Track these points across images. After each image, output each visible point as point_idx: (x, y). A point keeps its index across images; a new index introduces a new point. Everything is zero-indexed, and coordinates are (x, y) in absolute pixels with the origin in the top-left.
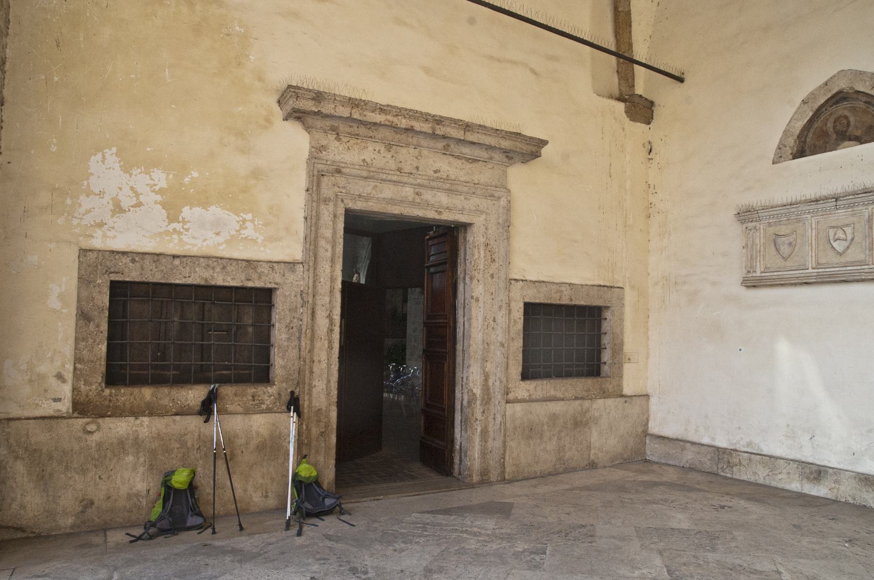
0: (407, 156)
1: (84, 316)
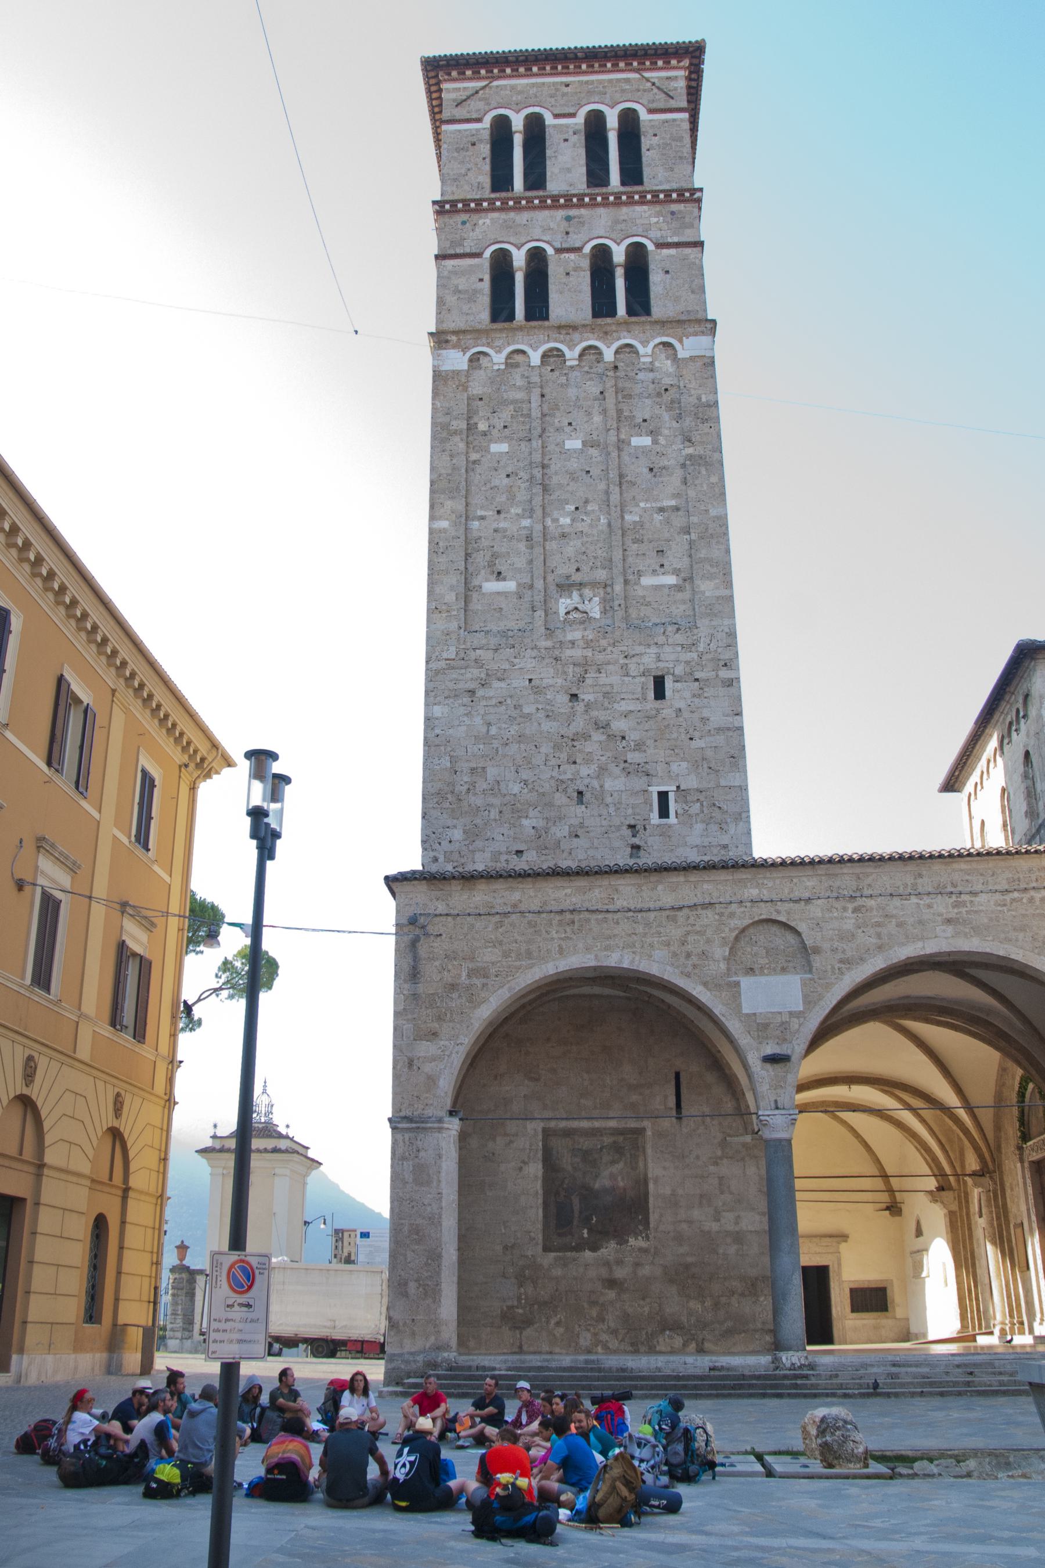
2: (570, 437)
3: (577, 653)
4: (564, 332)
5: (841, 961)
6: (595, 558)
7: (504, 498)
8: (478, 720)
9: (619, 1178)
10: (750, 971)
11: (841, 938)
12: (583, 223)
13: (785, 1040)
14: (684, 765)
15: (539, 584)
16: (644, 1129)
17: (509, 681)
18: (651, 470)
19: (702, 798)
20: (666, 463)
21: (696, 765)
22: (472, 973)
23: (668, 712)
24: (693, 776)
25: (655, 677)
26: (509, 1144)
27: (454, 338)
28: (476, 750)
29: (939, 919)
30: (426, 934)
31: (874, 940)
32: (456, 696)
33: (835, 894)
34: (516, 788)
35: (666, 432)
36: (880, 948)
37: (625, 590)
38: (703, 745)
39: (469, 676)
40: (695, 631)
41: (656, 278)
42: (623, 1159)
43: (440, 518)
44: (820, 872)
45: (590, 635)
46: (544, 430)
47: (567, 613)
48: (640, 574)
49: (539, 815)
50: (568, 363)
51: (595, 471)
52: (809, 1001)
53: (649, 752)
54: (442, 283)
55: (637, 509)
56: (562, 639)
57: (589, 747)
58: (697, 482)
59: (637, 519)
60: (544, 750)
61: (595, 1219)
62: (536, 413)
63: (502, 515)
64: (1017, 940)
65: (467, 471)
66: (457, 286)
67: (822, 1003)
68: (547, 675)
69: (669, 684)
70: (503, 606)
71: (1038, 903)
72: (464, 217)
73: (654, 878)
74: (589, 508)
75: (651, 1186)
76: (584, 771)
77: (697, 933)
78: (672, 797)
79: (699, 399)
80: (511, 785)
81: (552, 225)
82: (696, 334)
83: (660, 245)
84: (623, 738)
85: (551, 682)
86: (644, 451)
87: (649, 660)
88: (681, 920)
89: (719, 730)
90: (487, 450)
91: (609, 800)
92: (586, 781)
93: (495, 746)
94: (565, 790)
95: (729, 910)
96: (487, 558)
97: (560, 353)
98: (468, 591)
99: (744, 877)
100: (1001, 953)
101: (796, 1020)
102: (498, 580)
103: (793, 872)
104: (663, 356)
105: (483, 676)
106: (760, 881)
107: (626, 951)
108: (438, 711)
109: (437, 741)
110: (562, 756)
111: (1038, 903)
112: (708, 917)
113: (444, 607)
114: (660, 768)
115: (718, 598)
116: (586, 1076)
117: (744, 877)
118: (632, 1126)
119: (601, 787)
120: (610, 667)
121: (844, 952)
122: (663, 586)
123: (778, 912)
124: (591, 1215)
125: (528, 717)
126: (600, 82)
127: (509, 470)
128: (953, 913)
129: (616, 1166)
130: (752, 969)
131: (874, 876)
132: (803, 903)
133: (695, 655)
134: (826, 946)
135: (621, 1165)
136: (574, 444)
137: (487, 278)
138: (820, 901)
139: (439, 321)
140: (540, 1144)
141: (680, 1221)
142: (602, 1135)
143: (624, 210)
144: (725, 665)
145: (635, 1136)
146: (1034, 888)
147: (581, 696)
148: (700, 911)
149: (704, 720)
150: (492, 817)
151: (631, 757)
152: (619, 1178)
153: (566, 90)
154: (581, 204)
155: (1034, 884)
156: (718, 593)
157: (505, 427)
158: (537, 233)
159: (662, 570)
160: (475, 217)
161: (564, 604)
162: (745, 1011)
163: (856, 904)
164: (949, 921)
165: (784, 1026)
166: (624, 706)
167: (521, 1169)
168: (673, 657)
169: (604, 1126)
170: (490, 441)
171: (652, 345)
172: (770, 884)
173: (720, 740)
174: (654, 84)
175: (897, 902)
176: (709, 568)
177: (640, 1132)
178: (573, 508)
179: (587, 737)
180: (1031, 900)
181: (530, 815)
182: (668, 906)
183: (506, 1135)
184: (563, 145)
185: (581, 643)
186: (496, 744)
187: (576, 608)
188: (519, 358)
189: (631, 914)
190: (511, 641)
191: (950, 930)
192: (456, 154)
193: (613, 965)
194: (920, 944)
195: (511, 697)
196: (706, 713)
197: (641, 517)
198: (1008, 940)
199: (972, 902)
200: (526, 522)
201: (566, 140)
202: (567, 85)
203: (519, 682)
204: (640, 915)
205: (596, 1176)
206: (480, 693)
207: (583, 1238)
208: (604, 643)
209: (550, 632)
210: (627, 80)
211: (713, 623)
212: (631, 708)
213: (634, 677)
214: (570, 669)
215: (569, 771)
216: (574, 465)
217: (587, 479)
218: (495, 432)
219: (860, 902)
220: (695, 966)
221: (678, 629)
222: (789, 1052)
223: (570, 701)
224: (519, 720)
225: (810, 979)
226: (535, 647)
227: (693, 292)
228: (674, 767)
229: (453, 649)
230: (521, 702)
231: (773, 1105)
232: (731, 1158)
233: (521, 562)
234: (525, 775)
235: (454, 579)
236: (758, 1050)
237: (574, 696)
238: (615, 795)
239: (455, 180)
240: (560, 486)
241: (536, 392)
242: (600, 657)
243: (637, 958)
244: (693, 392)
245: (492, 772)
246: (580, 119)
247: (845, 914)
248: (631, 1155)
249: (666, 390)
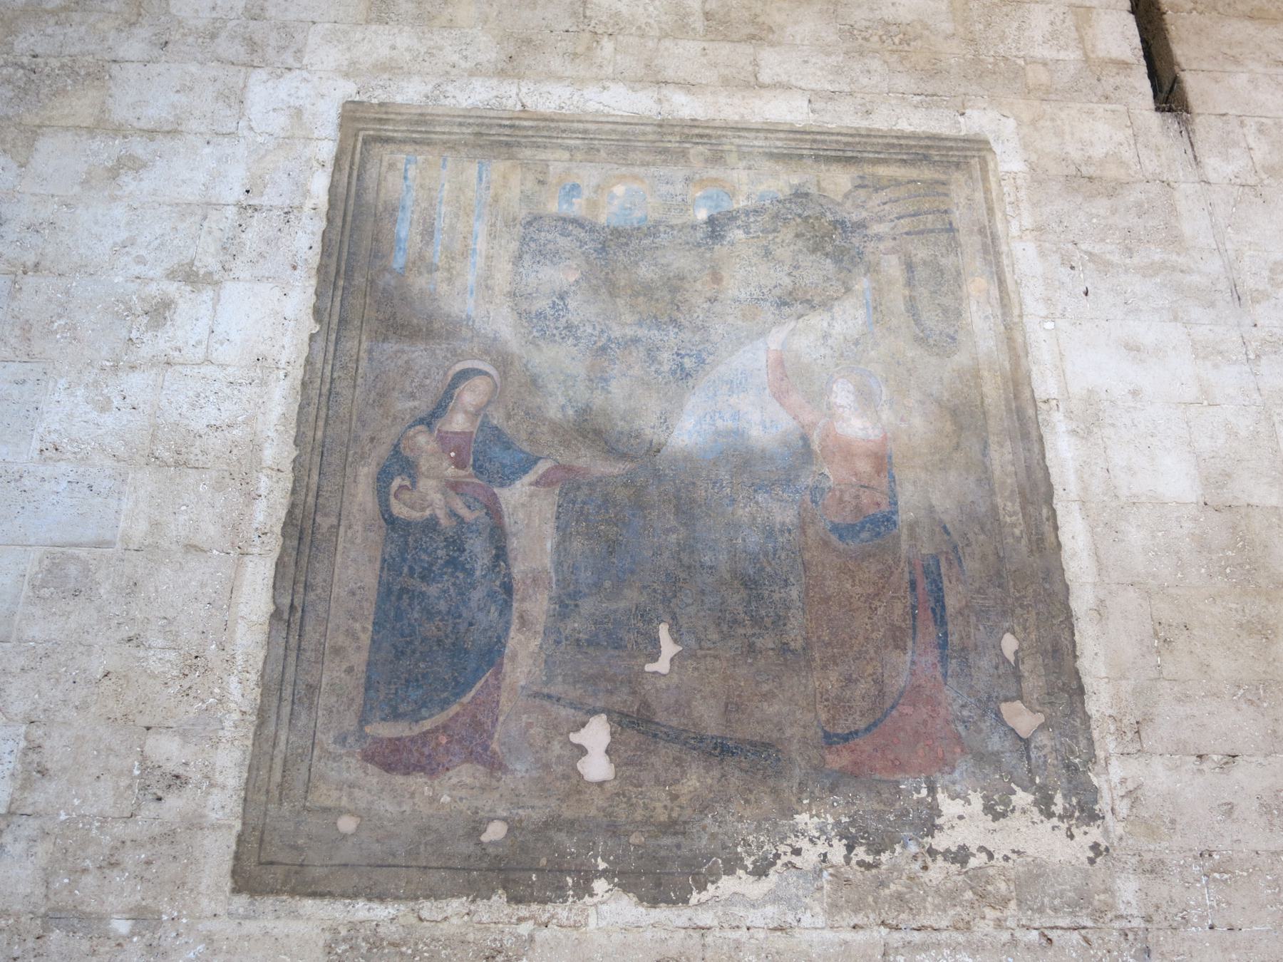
9: (842, 395)
26: (114, 173)
42: (863, 284)
61: (669, 648)
118: (904, 126)
124: (646, 616)
129: (818, 320)
140: (320, 184)
142: (717, 158)
145: (927, 173)
152: (842, 395)
167: (160, 312)
183: (102, 126)
205: (683, 375)
207: (578, 786)
248: (910, 267)
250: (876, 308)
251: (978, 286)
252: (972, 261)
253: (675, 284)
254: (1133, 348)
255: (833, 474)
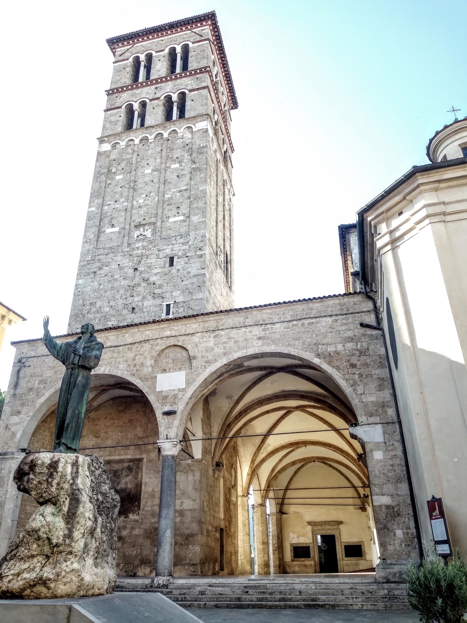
0: (323, 527)
1: (291, 551)
2: (147, 169)
3: (139, 252)
4: (148, 129)
5: (206, 362)
6: (151, 214)
7: (118, 196)
8: (96, 283)
10: (164, 371)
11: (207, 351)
12: (161, 89)
13: (175, 403)
14: (178, 292)
15: (127, 227)
16: (143, 459)
17: (110, 266)
18: (178, 176)
19: (184, 305)
20: (184, 173)
21: (183, 292)
22: (40, 382)
23: (174, 271)
24: (182, 297)
25: (170, 258)
27: (107, 139)
28: (93, 295)
29: (255, 337)
30: (25, 366)
31: (222, 351)
32: (89, 275)
33: (206, 330)
34: (107, 309)
35: (185, 161)
36: (225, 354)
37: (161, 225)
38: (187, 283)
39: (95, 266)
40: (188, 237)
41: (188, 103)
43: (92, 207)
44: (199, 321)
45: (145, 244)
46: (137, 168)
47: (138, 237)
48: (169, 217)
49: (115, 319)
50: (150, 141)
51: (156, 180)
52: (188, 383)
53: (164, 288)
54: (106, 120)
55: (170, 192)
56: (134, 247)
57: (140, 289)
58: (195, 178)
59: (170, 196)
60: (120, 292)
62: (134, 161)
63: (117, 202)
64: (294, 345)
65: (105, 188)
66: (111, 120)
67: (195, 383)
68: (127, 263)
69: (175, 260)
70: (113, 237)
71: (306, 326)
72: (117, 95)
73: (124, 331)
74: (151, 195)
75: (143, 487)
76: (136, 299)
77: (140, 354)
78: (172, 306)
79: (200, 145)
80: (105, 308)
81: (150, 91)
82: (201, 121)
83: (190, 91)
84: (154, 284)
85: (127, 264)
86: (176, 169)
87: (168, 251)
88: (134, 349)
89: (195, 276)
90: (115, 179)
91: (145, 310)
92: (136, 303)
93: (101, 293)
94: (127, 308)
95: (156, 342)
96: (109, 220)
97: (147, 138)
98: (100, 232)
99: (165, 326)
100: (286, 352)
101: (181, 393)
102: (112, 227)
103: (184, 321)
104: (187, 132)
105: (100, 265)
106: (172, 328)
107: (108, 366)
108: (80, 282)
109: (79, 294)
110: (128, 294)
111: (306, 326)
112: (147, 346)
113: (89, 241)
114: (168, 295)
115: (199, 222)
116: (120, 434)
117: (165, 326)
119: (143, 305)
120: (151, 256)
121: (207, 357)
122: (178, 221)
123: (178, 341)
125: (116, 280)
126: (175, 37)
127: (122, 185)
128: (262, 334)
130: (165, 370)
131: (225, 320)
132: (190, 335)
133: (187, 247)
134: (199, 355)
135: (130, 477)
136: (148, 171)
137: (122, 115)
138: (198, 334)
139: (103, 134)
141: (155, 505)
142: (123, 463)
143: (179, 81)
144: (200, 249)
146: (304, 318)
147: (139, 269)
148: (143, 344)
149: (189, 273)
150: (96, 322)
151: (156, 291)
152: (129, 484)
153: (162, 42)
154: (162, 82)
155: (305, 317)
156: (199, 220)
157: (123, 169)
158: (144, 95)
159: (178, 215)
160: (121, 94)
161: (137, 233)
162: (158, 390)
163: (215, 334)
164: (260, 338)
165: (175, 396)
166: (156, 271)
168: (178, 248)
169: (125, 458)
170: (116, 175)
171: (183, 128)
172: (176, 328)
173: (195, 280)
174: (196, 33)
175: (235, 331)
176: (197, 211)
177: (140, 460)
178: (145, 196)
179: (139, 285)
180: (303, 324)
181: (112, 320)
182: (129, 343)
184: (158, 62)
185: (141, 248)
186: (102, 292)
187: (141, 234)
188: (131, 143)
189: (112, 348)
190: (113, 250)
191: (260, 342)
192: (117, 73)
193: (101, 373)
194: (245, 351)
195: (110, 272)
196: (189, 270)
197: (172, 195)
198: (290, 345)
199: (272, 328)
200: (125, 204)
201: (160, 60)
202: (163, 41)
203: (114, 266)
204: (116, 348)
205: (119, 483)
206: (98, 273)
208: (150, 246)
209: (129, 245)
210: (186, 34)
211: (196, 233)
212: (159, 271)
213: (161, 259)
214: (135, 259)
215: (130, 299)
216: (147, 179)
217: (152, 184)
218: (118, 172)
219: (217, 333)
220: (137, 370)
221: (182, 237)
222: (176, 410)
223: (134, 271)
224: (112, 281)
225: (190, 372)
226: (123, 252)
227: (202, 106)
228: (174, 294)
229: (90, 257)
230: (114, 274)
231: (165, 438)
232: (182, 471)
233: (122, 220)
234: (112, 303)
235: (95, 230)
236: (161, 409)
237: (136, 269)
238: (148, 308)
239: (116, 82)
240: (141, 188)
241: (135, 154)
242: (148, 252)
243: (112, 369)
244: (197, 143)
245: (98, 304)
246: (167, 51)
247: (209, 339)
249: (187, 145)
250: (132, 476)
251: (140, 473)
252: (140, 471)
253: (119, 475)
254: (150, 478)
255: (128, 491)
